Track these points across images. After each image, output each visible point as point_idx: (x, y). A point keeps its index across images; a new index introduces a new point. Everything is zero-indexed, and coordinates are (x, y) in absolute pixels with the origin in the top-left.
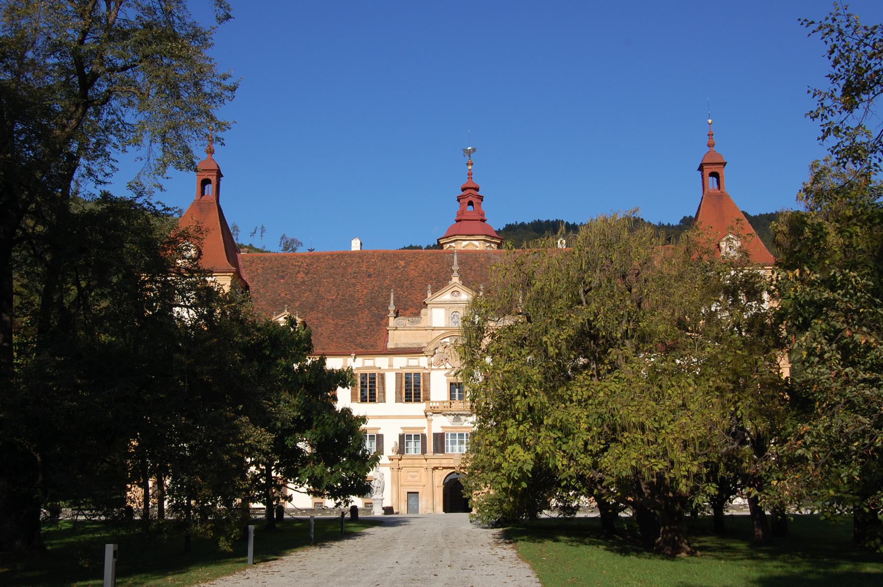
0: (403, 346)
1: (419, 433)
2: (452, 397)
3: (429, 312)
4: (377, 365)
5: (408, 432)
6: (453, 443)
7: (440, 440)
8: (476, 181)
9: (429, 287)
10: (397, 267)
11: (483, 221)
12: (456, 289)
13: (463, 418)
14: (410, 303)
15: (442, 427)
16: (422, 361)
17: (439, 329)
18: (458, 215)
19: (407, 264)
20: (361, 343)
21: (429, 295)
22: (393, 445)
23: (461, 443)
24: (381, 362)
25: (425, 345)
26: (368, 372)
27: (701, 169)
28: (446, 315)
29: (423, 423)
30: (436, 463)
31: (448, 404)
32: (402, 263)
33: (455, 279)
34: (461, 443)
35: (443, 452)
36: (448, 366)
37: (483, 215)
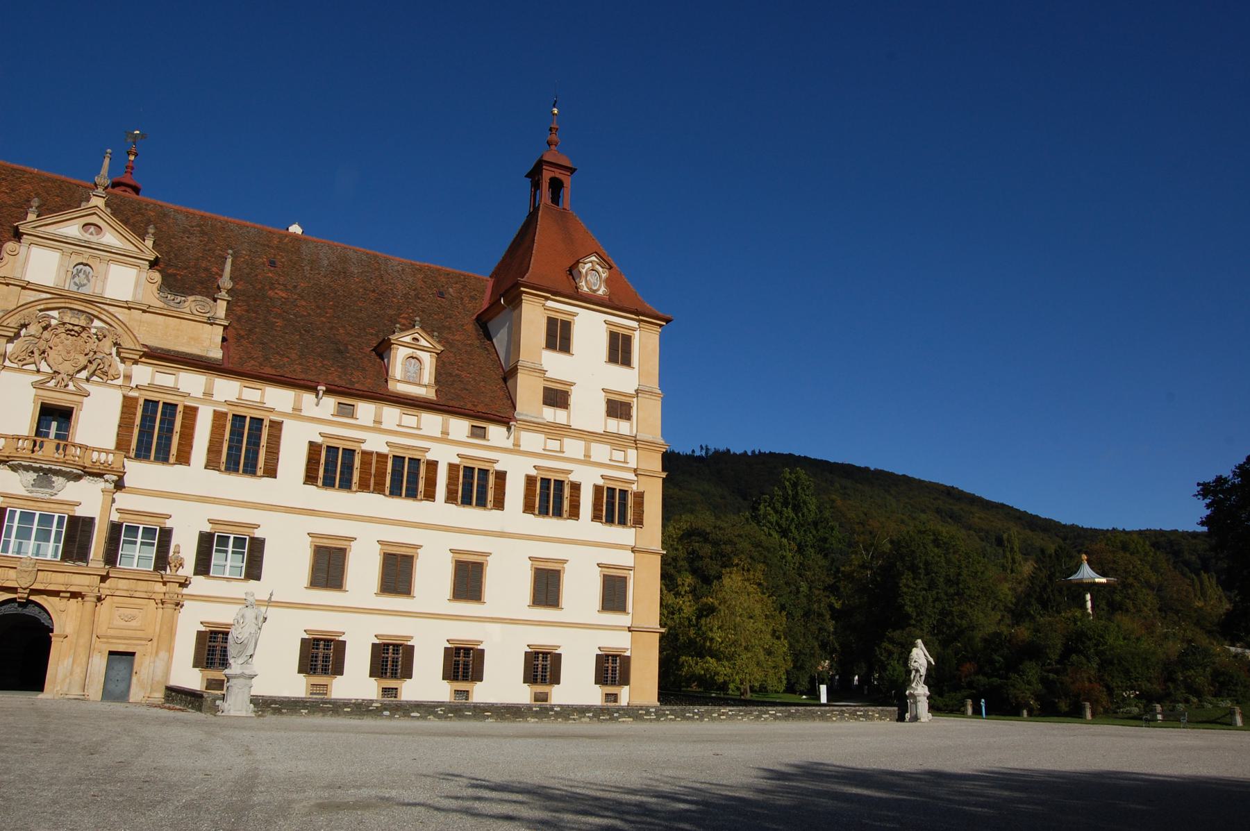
3: (22, 248)
6: (24, 534)
9: (35, 202)
12: (94, 219)
13: (58, 481)
21: (31, 217)
23: (44, 536)
27: (535, 175)
28: (61, 265)
31: (28, 445)
33: (98, 202)
34: (44, 536)
36: (44, 367)
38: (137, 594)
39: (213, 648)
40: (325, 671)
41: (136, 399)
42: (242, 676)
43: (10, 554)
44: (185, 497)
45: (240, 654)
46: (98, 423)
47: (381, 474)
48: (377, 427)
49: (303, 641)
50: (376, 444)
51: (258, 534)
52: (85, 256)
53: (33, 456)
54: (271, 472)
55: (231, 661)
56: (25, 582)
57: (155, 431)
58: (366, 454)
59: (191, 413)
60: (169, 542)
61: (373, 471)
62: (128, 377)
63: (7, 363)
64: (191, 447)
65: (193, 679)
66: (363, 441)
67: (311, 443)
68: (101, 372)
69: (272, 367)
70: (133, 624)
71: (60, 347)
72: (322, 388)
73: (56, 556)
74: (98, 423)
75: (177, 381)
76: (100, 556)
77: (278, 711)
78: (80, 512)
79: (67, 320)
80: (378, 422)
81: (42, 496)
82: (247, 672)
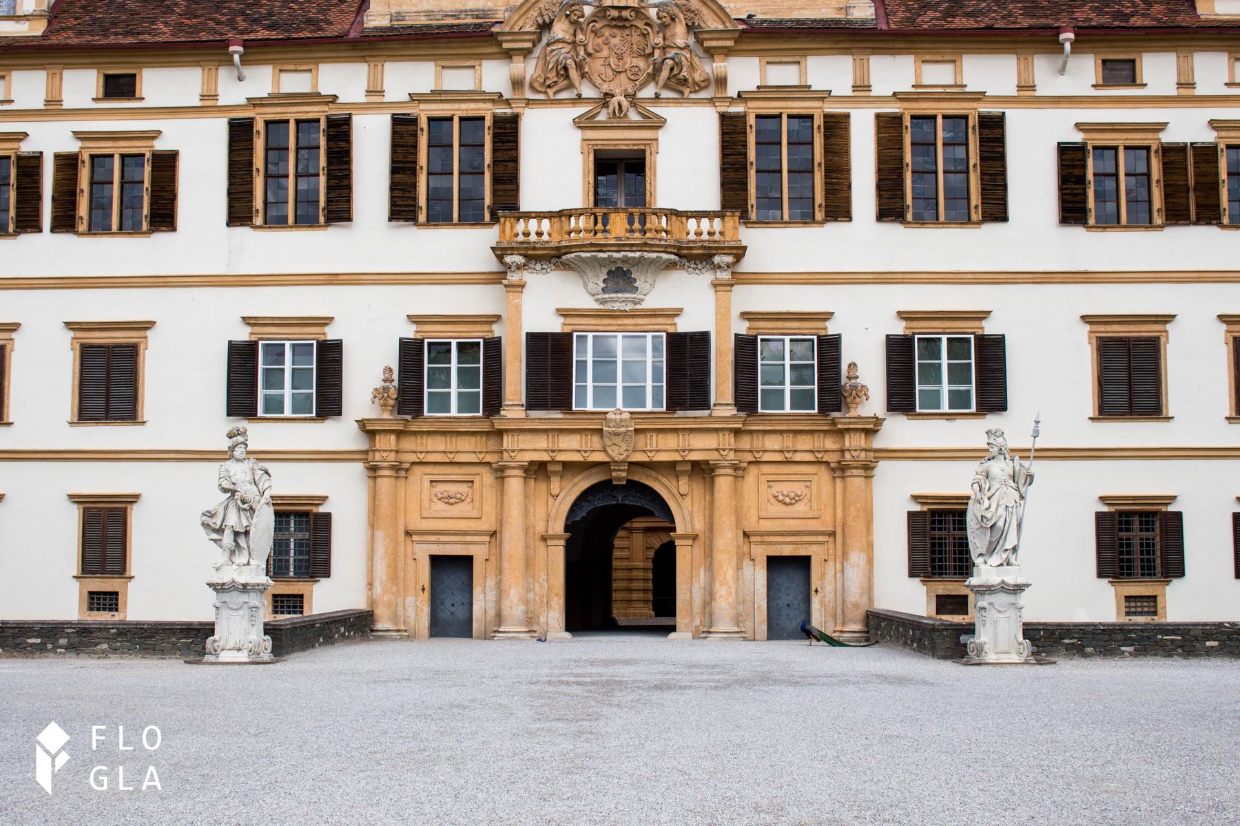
0: (423, 21)
1: (476, 335)
2: (600, 199)
4: (325, 90)
5: (434, 334)
7: (551, 358)
15: (565, 313)
16: (494, 76)
20: (270, 14)
22: (375, 380)
24: (342, 81)
25: (500, 16)
26: (293, 113)
30: (534, 448)
35: (562, 400)
36: (588, 91)
38: (798, 457)
39: (940, 538)
40: (1148, 571)
41: (742, 118)
42: (1004, 588)
43: (590, 407)
44: (853, 276)
45: (991, 551)
46: (685, 168)
47: (1209, 187)
48: (1186, 95)
49: (1100, 517)
50: (1188, 127)
51: (990, 328)
54: (996, 210)
55: (978, 561)
56: (618, 452)
57: (778, 168)
58: (1173, 153)
59: (837, 127)
60: (838, 359)
61: (1192, 182)
62: (722, 82)
63: (530, 95)
64: (850, 186)
65: (912, 599)
66: (1160, 127)
67: (1065, 150)
68: (681, 86)
69: (967, 15)
70: (800, 509)
71: (605, 53)
72: (1067, 36)
73: (657, 401)
74: (685, 168)
75: (804, 73)
76: (729, 397)
77: (1078, 650)
78: (684, 325)
80: (1186, 83)
81: (622, 307)
82: (1011, 580)
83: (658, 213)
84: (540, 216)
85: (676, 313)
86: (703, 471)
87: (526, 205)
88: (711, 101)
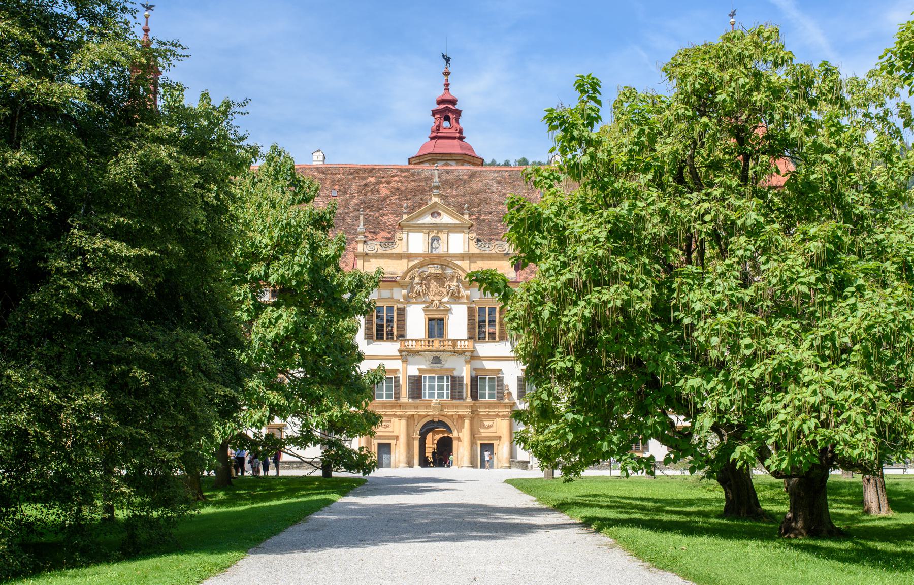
2: (431, 334)
3: (405, 235)
6: (432, 388)
7: (416, 384)
8: (454, 93)
10: (366, 185)
11: (461, 138)
14: (382, 226)
16: (399, 294)
17: (416, 256)
18: (433, 132)
19: (379, 181)
21: (405, 217)
23: (441, 388)
29: (397, 364)
32: (373, 180)
37: (461, 131)
46: (457, 325)
52: (435, 232)
53: (431, 348)
68: (456, 298)
74: (457, 325)
78: (456, 374)
79: (433, 271)
83: (449, 340)
84: (412, 340)
85: (454, 369)
86: (462, 418)
87: (408, 337)
88: (464, 303)
